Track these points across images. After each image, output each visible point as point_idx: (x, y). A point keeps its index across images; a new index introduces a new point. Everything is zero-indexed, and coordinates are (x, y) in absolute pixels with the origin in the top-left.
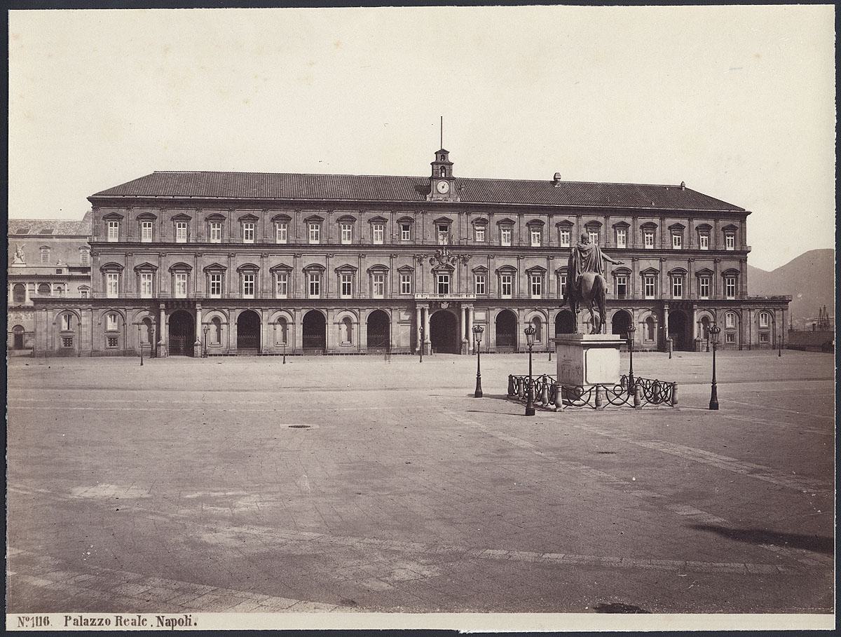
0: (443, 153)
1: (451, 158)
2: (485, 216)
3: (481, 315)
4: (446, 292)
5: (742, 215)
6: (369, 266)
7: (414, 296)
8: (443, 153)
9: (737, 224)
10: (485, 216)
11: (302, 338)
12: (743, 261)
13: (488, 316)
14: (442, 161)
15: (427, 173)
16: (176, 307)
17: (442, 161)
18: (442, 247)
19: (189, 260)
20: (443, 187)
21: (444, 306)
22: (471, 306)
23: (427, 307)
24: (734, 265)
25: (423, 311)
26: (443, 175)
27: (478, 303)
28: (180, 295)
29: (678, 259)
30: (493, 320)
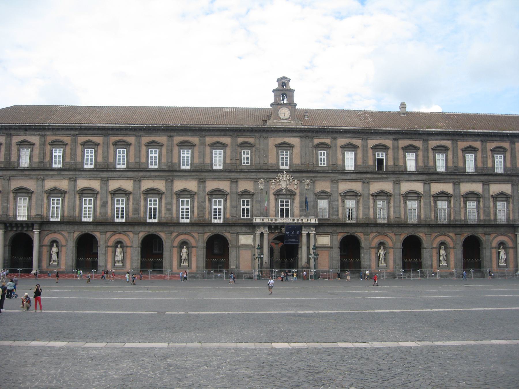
0: (283, 82)
1: (292, 85)
2: (328, 141)
3: (324, 240)
4: (287, 216)
7: (252, 220)
8: (283, 82)
10: (328, 141)
11: (139, 261)
13: (331, 240)
14: (284, 90)
15: (271, 99)
16: (15, 229)
17: (284, 90)
18: (282, 172)
19: (30, 185)
20: (285, 113)
22: (313, 231)
23: (266, 231)
25: (262, 234)
26: (285, 101)
27: (321, 226)
28: (22, 215)
30: (337, 244)
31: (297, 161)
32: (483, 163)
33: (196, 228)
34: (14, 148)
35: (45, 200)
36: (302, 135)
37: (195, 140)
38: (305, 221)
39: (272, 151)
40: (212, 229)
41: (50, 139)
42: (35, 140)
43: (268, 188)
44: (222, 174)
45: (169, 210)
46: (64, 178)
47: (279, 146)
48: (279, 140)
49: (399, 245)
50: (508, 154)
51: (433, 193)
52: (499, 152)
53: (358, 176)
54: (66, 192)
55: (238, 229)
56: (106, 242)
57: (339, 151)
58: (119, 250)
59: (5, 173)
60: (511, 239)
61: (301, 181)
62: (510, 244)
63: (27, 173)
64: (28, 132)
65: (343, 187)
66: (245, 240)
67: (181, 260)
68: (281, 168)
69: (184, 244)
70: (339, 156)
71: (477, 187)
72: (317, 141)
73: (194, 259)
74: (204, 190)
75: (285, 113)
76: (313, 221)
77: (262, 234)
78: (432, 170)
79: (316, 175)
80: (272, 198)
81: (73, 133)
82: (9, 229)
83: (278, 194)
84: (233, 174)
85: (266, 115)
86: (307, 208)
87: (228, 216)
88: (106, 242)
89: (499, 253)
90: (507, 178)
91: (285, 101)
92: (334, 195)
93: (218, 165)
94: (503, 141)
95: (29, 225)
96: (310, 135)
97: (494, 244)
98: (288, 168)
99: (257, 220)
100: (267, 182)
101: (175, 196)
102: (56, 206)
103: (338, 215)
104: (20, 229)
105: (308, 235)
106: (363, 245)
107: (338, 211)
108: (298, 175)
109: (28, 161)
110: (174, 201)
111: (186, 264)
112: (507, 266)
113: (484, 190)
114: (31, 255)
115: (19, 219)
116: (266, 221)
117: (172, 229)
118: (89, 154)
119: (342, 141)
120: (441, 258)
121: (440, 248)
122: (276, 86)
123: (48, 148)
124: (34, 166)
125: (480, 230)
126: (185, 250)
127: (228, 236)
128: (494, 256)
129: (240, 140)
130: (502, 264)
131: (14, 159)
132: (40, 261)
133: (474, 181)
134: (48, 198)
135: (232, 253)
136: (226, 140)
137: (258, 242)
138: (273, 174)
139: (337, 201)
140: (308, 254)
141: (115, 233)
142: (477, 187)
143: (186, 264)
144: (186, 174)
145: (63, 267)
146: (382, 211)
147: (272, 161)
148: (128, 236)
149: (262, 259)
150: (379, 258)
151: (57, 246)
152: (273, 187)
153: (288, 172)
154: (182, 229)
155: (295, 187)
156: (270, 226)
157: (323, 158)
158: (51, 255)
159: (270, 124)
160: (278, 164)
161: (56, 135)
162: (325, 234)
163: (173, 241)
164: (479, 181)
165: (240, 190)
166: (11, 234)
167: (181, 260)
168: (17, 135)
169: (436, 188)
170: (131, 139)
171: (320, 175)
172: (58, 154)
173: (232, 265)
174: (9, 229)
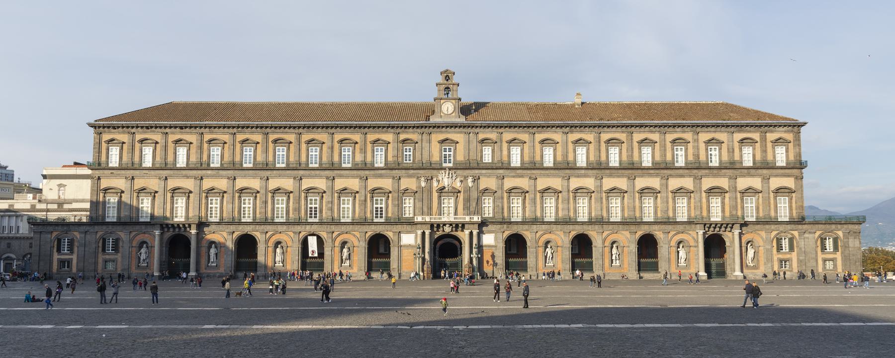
0: (447, 76)
1: (455, 79)
3: (488, 239)
5: (796, 126)
6: (369, 188)
8: (447, 76)
9: (789, 136)
12: (799, 178)
13: (496, 239)
14: (448, 84)
15: (434, 92)
16: (171, 230)
17: (448, 84)
21: (447, 229)
24: (789, 183)
25: (423, 233)
28: (180, 217)
29: (715, 176)
31: (460, 157)
32: (661, 156)
33: (357, 227)
34: (171, 146)
35: (204, 201)
36: (465, 130)
37: (357, 137)
38: (467, 219)
39: (435, 147)
40: (373, 227)
41: (207, 137)
42: (192, 137)
43: (431, 187)
44: (383, 172)
45: (332, 209)
46: (222, 177)
47: (443, 142)
48: (442, 137)
49: (568, 245)
50: (690, 146)
51: (604, 189)
52: (680, 144)
53: (525, 171)
54: (225, 192)
55: (399, 228)
56: (267, 241)
57: (505, 145)
58: (278, 250)
59: (161, 172)
60: (693, 238)
61: (466, 178)
62: (692, 243)
63: (184, 172)
64: (184, 130)
65: (509, 183)
66: (409, 239)
67: (342, 260)
68: (444, 165)
69: (344, 243)
70: (505, 152)
71: (654, 182)
72: (481, 136)
73: (355, 258)
74: (366, 187)
75: (448, 108)
76: (476, 219)
77: (423, 233)
78: (603, 166)
79: (480, 171)
80: (435, 195)
81: (231, 130)
82: (166, 230)
83: (441, 190)
84: (394, 172)
85: (430, 110)
86: (473, 203)
87: (390, 215)
88: (267, 241)
89: (678, 252)
90: (687, 171)
91: (450, 96)
92: (498, 194)
93: (380, 162)
94: (684, 132)
95: (186, 226)
96: (474, 130)
97: (673, 243)
98: (451, 165)
99: (419, 219)
100: (429, 180)
101: (336, 195)
102: (214, 206)
103: (503, 213)
104: (177, 230)
105: (471, 233)
106: (528, 244)
107: (503, 209)
108: (459, 172)
109: (185, 160)
110: (336, 201)
111: (347, 263)
112: (687, 267)
113: (661, 185)
114: (188, 256)
115: (176, 220)
116: (428, 219)
117: (333, 228)
118: (248, 153)
119: (508, 135)
120: (614, 258)
121: (612, 248)
122: (441, 79)
123: (206, 146)
124: (191, 166)
125: (656, 227)
126: (345, 250)
127: (390, 235)
128: (673, 256)
129: (402, 137)
130: (682, 263)
131: (170, 159)
132: (198, 263)
133: (651, 175)
134: (207, 197)
135: (394, 252)
136: (389, 137)
137: (419, 241)
138: (435, 171)
139: (502, 198)
140: (471, 252)
141: (276, 232)
142: (654, 182)
143: (347, 263)
144: (347, 172)
145: (222, 270)
146: (550, 209)
147: (436, 158)
148: (287, 235)
149: (424, 259)
150: (546, 257)
151: (216, 247)
152: (435, 184)
153: (450, 169)
154: (343, 228)
155: (458, 185)
156: (432, 226)
157: (487, 155)
158: (209, 256)
159: (434, 120)
160: (441, 160)
161: (212, 133)
162: (490, 232)
163: (334, 241)
164: (657, 175)
165: (403, 187)
166: (168, 235)
167: (342, 260)
168: (173, 133)
169: (609, 183)
170: (291, 137)
171: (484, 171)
172: (215, 153)
173: (394, 265)
174: (166, 230)
